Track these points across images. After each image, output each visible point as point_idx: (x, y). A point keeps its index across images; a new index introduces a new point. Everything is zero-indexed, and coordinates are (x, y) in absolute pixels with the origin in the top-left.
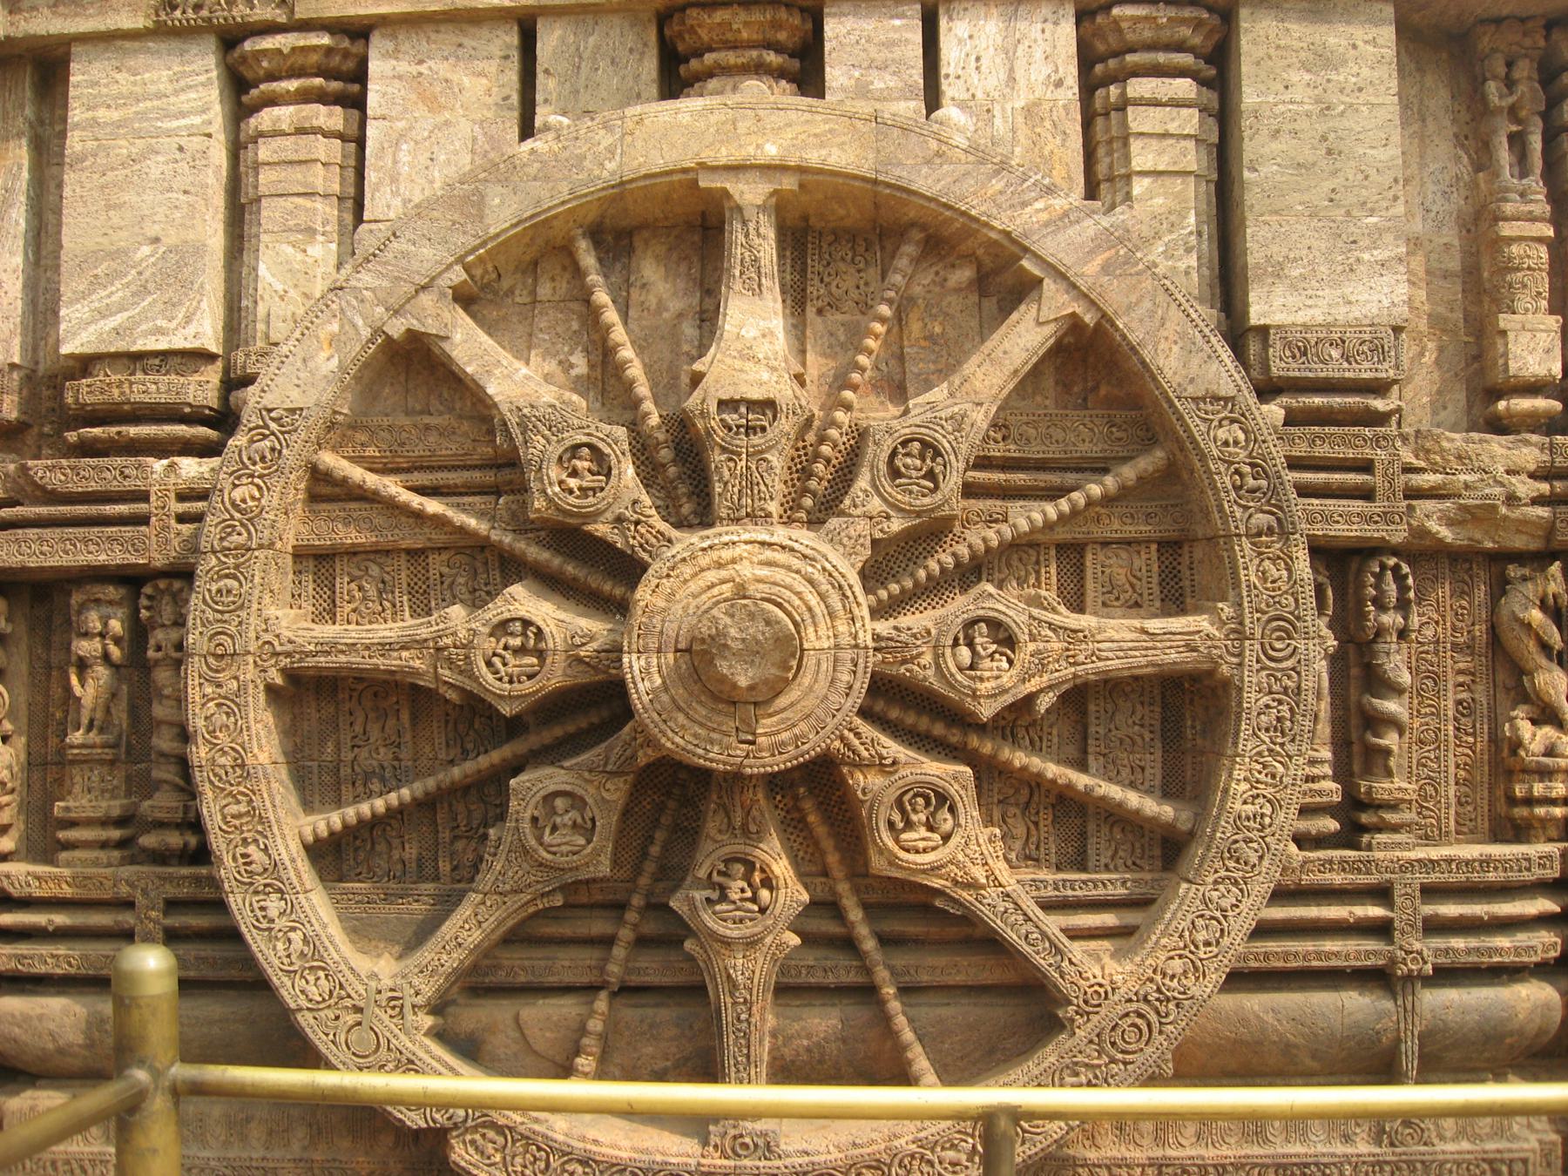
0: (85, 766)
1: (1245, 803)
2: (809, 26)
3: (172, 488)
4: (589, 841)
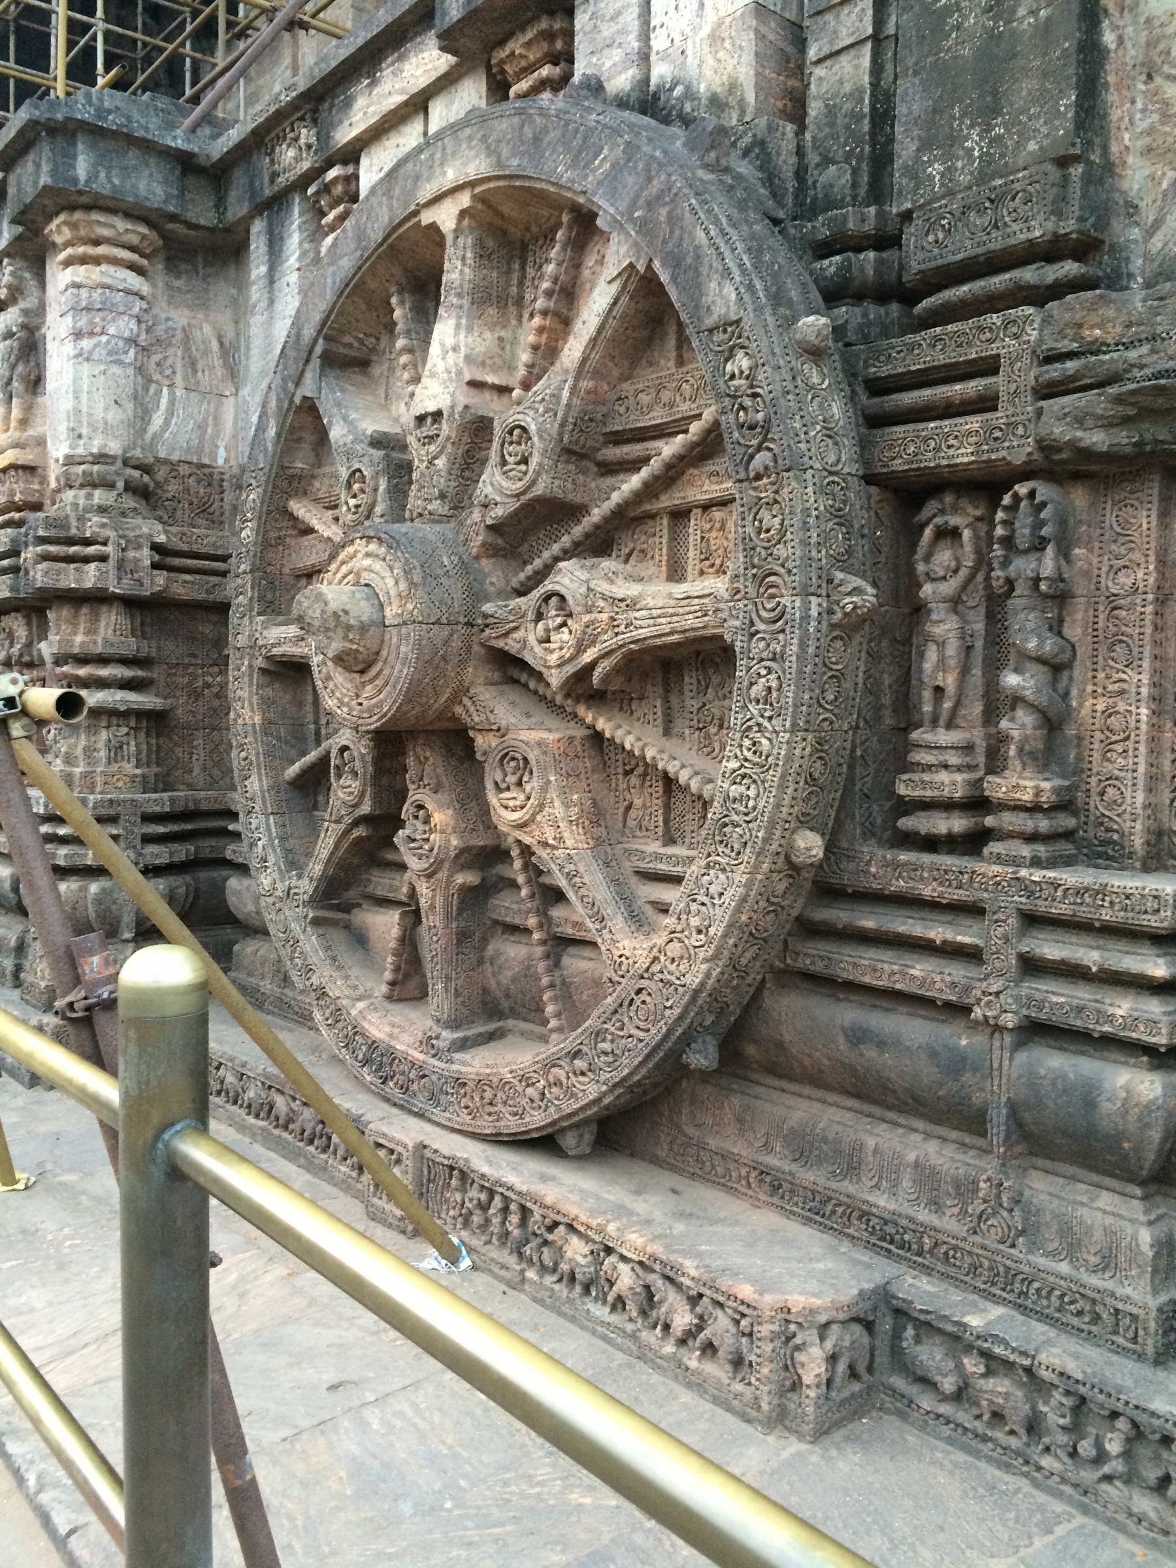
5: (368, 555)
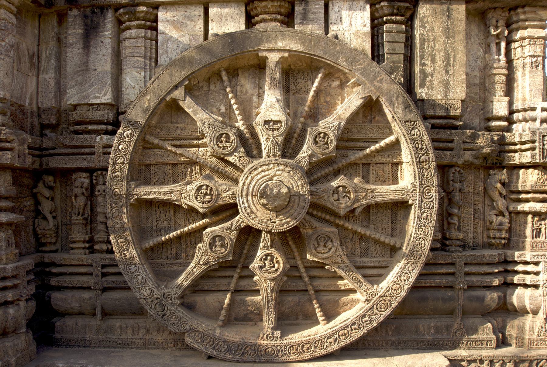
0: (78, 225)
1: (417, 240)
2: (291, 7)
3: (101, 144)
4: (226, 250)
5: (278, 170)
